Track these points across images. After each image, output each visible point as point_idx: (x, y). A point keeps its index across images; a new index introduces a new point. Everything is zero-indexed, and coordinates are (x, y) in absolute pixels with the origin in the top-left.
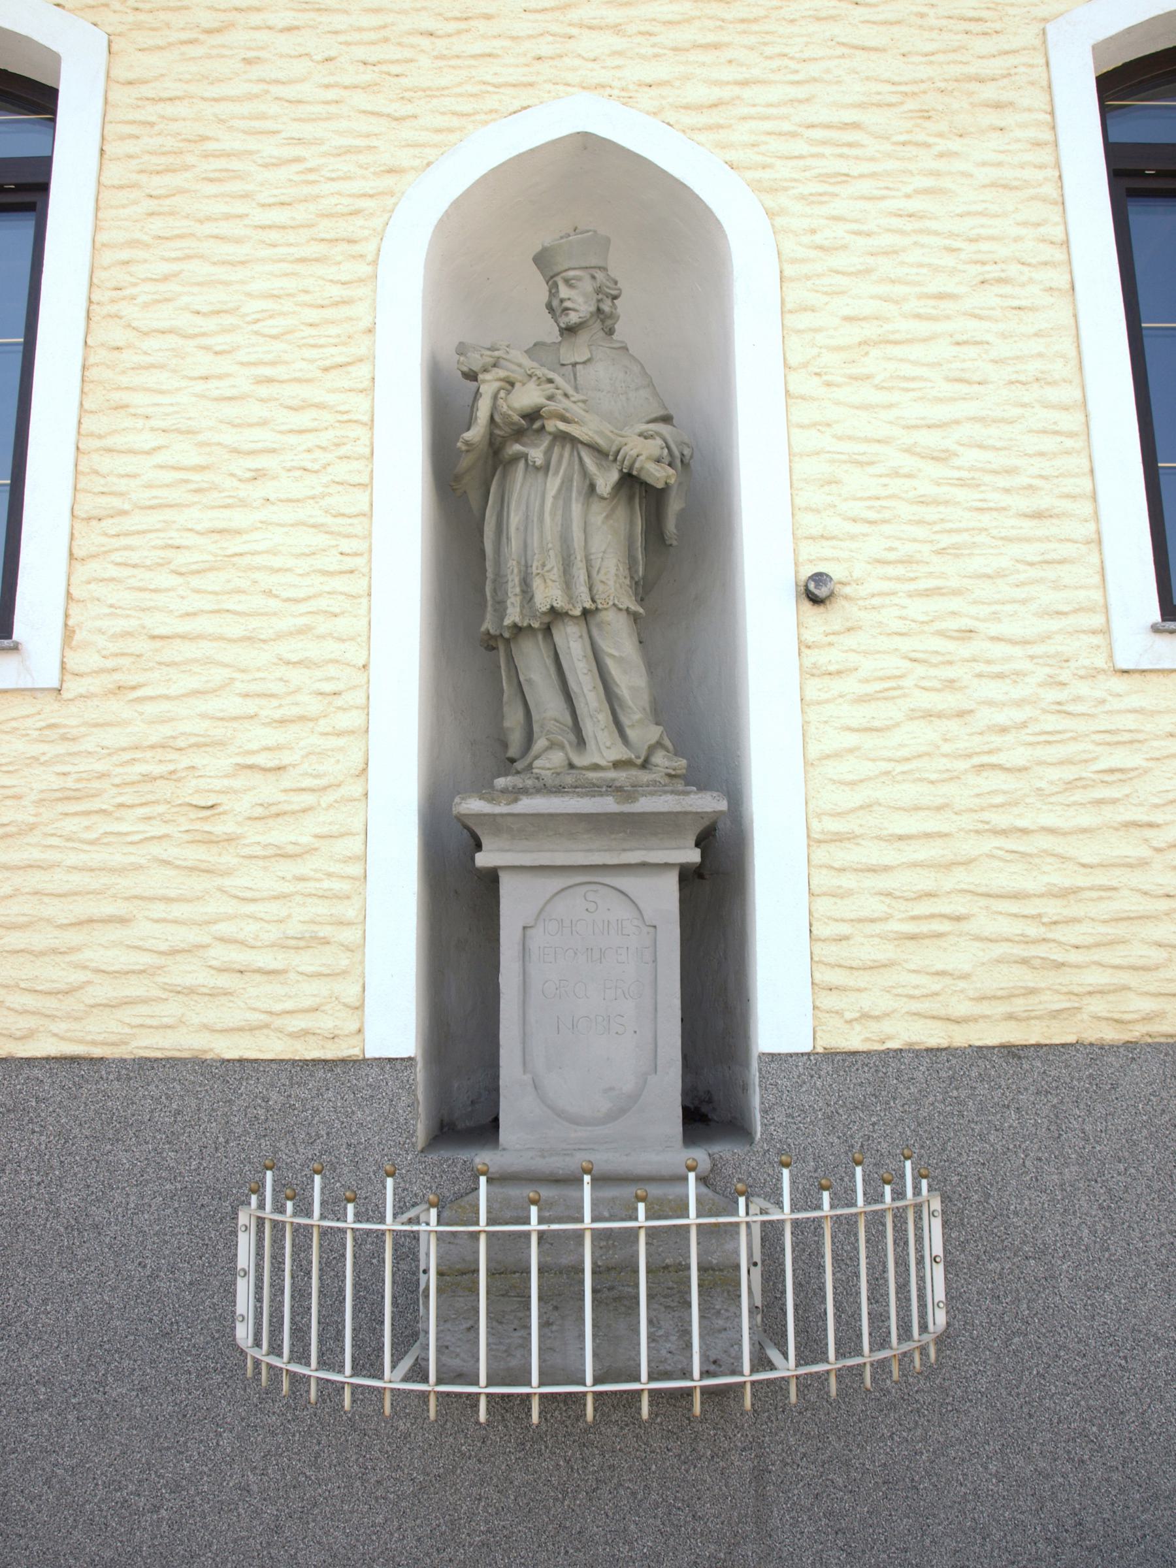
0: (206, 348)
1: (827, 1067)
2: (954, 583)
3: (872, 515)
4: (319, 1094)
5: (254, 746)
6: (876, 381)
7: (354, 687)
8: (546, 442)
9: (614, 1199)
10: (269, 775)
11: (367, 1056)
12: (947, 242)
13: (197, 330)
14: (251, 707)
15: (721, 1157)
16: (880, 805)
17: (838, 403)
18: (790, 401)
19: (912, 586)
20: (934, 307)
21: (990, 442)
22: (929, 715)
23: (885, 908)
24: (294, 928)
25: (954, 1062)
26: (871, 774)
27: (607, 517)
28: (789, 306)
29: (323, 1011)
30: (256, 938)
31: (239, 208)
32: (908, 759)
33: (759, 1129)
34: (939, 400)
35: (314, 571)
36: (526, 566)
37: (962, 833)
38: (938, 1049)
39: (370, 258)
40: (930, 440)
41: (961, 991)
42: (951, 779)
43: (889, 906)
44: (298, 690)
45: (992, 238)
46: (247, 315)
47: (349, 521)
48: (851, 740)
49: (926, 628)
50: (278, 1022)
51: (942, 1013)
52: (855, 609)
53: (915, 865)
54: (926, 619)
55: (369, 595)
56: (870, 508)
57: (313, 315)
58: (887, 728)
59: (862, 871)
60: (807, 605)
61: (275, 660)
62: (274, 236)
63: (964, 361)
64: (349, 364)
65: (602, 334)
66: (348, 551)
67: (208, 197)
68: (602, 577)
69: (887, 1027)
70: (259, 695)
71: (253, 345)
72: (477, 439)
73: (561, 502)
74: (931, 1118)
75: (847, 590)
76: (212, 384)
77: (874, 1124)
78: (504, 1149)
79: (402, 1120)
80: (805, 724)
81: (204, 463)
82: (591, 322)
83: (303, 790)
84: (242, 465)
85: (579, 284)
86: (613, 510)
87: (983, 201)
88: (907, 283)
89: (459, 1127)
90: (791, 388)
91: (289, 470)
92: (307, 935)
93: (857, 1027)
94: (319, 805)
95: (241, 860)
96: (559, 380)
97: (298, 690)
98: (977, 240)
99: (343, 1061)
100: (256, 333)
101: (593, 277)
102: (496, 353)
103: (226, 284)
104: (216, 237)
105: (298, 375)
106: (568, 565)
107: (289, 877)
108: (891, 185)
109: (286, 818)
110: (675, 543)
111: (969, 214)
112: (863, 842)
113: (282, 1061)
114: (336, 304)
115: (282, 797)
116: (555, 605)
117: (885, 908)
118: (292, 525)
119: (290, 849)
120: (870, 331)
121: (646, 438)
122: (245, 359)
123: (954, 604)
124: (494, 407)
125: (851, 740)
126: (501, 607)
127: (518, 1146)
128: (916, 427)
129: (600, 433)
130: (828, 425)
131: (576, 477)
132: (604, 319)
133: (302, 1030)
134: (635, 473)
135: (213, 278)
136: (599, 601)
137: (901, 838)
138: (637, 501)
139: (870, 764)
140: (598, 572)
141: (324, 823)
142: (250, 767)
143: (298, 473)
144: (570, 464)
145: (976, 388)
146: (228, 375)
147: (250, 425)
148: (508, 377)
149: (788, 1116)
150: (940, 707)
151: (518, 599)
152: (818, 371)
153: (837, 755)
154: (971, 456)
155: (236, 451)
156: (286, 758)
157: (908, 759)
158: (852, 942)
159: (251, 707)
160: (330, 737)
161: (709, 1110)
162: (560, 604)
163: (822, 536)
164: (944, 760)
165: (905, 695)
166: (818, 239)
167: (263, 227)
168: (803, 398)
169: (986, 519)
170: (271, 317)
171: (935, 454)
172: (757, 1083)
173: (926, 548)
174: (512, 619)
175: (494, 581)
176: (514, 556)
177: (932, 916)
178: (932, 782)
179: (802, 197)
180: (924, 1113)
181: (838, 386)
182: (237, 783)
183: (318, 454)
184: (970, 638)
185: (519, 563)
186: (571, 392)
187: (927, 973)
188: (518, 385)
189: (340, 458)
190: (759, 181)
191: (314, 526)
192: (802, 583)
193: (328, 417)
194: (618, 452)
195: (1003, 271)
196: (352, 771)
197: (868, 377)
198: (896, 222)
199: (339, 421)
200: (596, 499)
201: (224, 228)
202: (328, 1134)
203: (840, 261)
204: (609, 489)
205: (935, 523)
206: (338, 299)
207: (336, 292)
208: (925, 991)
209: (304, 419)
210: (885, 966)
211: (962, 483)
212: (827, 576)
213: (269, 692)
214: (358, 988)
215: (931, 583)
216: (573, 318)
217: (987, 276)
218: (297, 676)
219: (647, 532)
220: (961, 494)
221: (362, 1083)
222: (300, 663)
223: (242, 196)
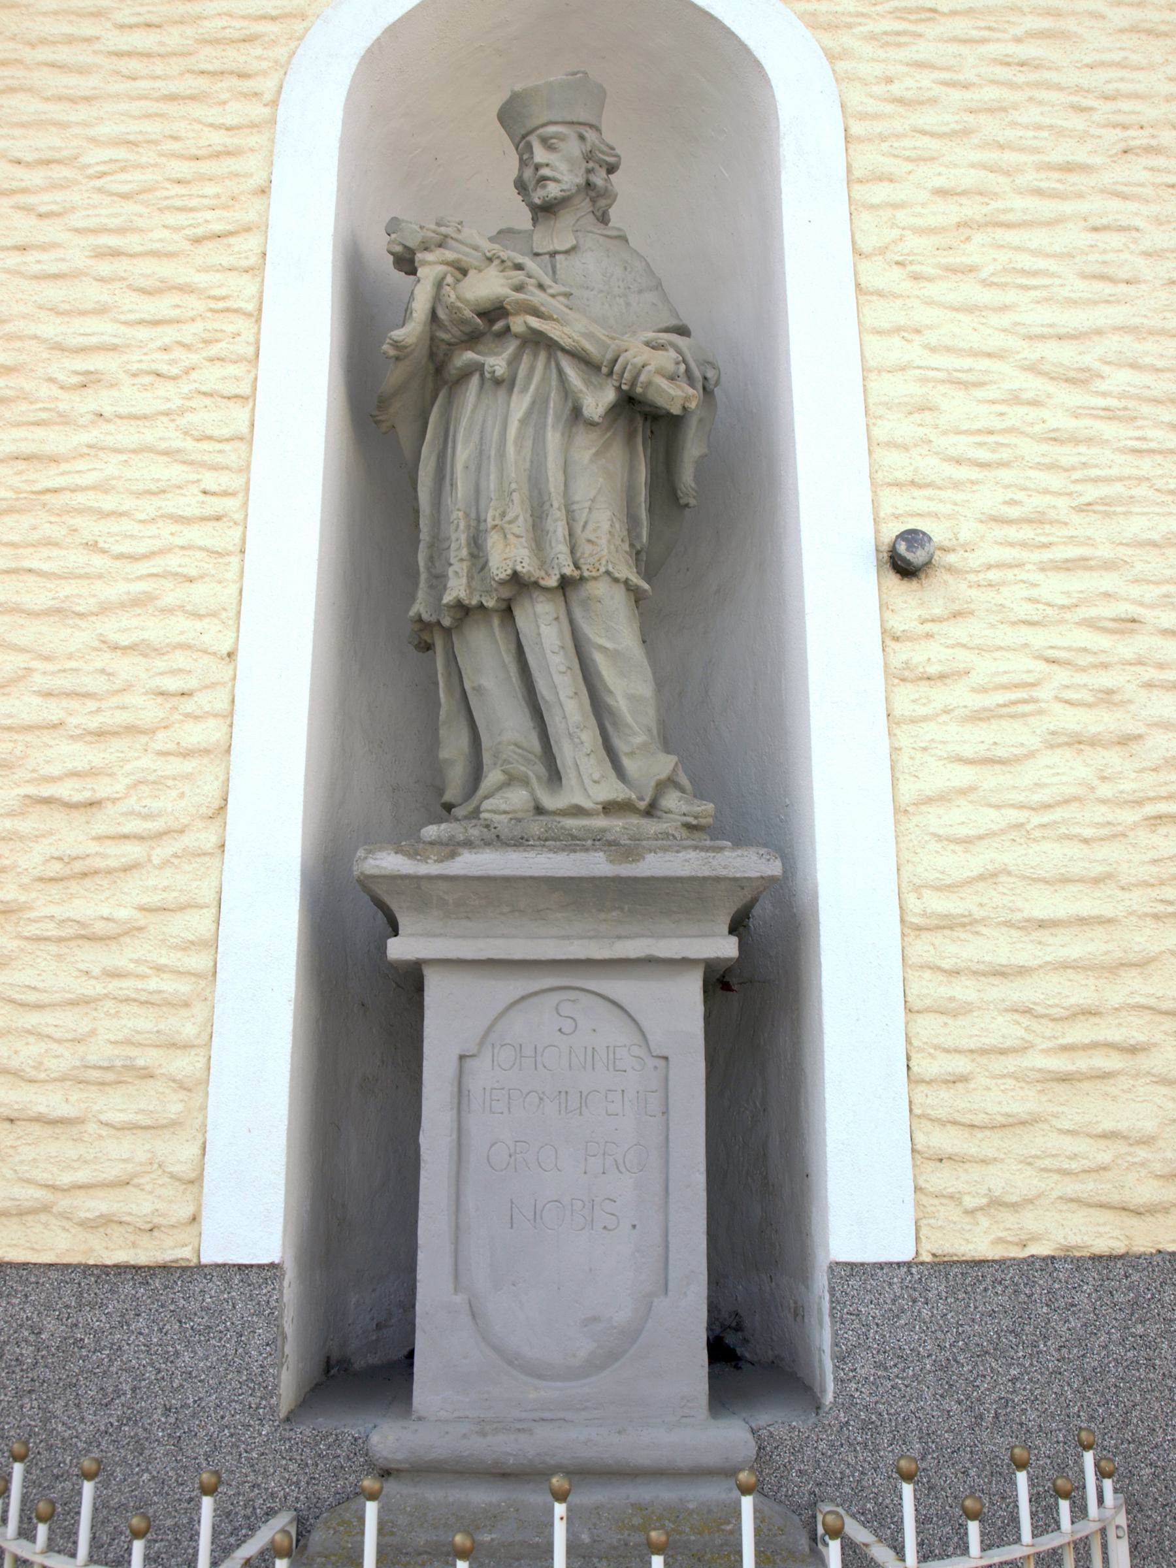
0: (28, 209)
1: (937, 1286)
2: (1105, 552)
3: (983, 455)
4: (124, 1323)
5: (55, 770)
6: (983, 275)
7: (213, 685)
8: (511, 347)
9: (598, 1508)
10: (75, 814)
11: (204, 1261)
12: (1074, 99)
13: (15, 185)
14: (54, 711)
15: (771, 1435)
16: (1009, 873)
17: (930, 303)
18: (862, 299)
19: (1046, 555)
20: (1059, 181)
21: (1148, 360)
22: (1078, 741)
23: (1021, 1033)
24: (99, 1051)
25: (1135, 1277)
26: (995, 827)
27: (596, 454)
28: (857, 174)
29: (137, 1186)
30: (39, 1066)
31: (88, 28)
32: (1048, 806)
33: (830, 1386)
34: (1071, 303)
35: (162, 516)
36: (478, 520)
37: (1134, 919)
38: (1110, 1257)
39: (268, 96)
40: (1063, 355)
41: (1142, 1164)
42: (1114, 836)
43: (1027, 1029)
44: (127, 688)
45: (1136, 96)
46: (89, 166)
47: (219, 446)
48: (963, 776)
49: (1068, 616)
50: (64, 1203)
51: (1116, 1198)
52: (963, 586)
53: (1065, 966)
54: (1066, 601)
55: (243, 552)
56: (980, 444)
57: (183, 169)
58: (1017, 760)
59: (984, 974)
60: (893, 579)
61: (96, 644)
62: (133, 65)
63: (1105, 252)
64: (231, 233)
65: (591, 218)
66: (213, 487)
67: (45, 14)
68: (589, 534)
69: (1030, 1221)
70: (68, 695)
71: (95, 207)
72: (411, 340)
73: (530, 431)
74: (1103, 1370)
75: (951, 558)
76: (31, 257)
77: (1014, 1380)
78: (420, 1419)
79: (255, 1368)
80: (895, 750)
81: (10, 362)
82: (576, 201)
83: (126, 837)
84: (66, 367)
85: (562, 145)
86: (606, 446)
87: (1121, 49)
88: (1022, 150)
89: (357, 1366)
90: (863, 280)
91: (134, 375)
92: (118, 1063)
93: (984, 1221)
94: (150, 861)
95: (22, 943)
96: (530, 264)
97: (127, 688)
98: (1114, 99)
99: (165, 1268)
100: (100, 190)
101: (582, 138)
102: (443, 230)
103: (64, 125)
104: (53, 65)
105: (157, 246)
106: (540, 518)
107: (96, 971)
108: (994, 25)
109: (97, 879)
110: (692, 502)
111: (1102, 64)
112: (984, 930)
113: (67, 1266)
114: (217, 155)
115: (93, 847)
116: (519, 568)
117: (1021, 1033)
118: (134, 451)
119: (100, 928)
120: (972, 209)
121: (653, 348)
122: (81, 224)
123: (1108, 581)
124: (437, 298)
125: (963, 776)
126: (439, 581)
127: (443, 1414)
128: (1042, 337)
129: (589, 336)
130: (918, 331)
131: (554, 396)
132: (595, 197)
133: (101, 1216)
134: (639, 390)
135: (44, 117)
136: (584, 568)
137: (1042, 924)
138: (639, 439)
139: (993, 813)
140: (584, 527)
141: (155, 888)
142: (47, 801)
143: (147, 379)
144: (545, 379)
145: (1123, 288)
146: (55, 245)
147: (83, 313)
148: (458, 261)
149: (878, 1365)
150: (1093, 730)
151: (465, 565)
152: (900, 259)
153: (942, 798)
154: (1120, 379)
155: (59, 347)
156: (103, 788)
157: (1048, 806)
158: (972, 1085)
159: (54, 711)
160: (171, 758)
161: (745, 1353)
162: (527, 567)
163: (913, 483)
164: (1103, 809)
165: (1041, 712)
166: (896, 89)
167: (119, 54)
168: (880, 294)
169: (1146, 465)
170: (123, 170)
171: (1071, 374)
172: (826, 1306)
173: (1062, 503)
174: (454, 594)
175: (431, 546)
176: (460, 505)
177: (1094, 1046)
178: (1086, 841)
179: (872, 37)
180: (1092, 1362)
181: (930, 279)
182: (24, 826)
183: (179, 353)
184: (1132, 631)
185: (467, 515)
186: (547, 281)
187: (1089, 1135)
188: (472, 273)
189: (211, 360)
190: (814, 14)
191: (166, 453)
192: (885, 548)
193: (195, 304)
194: (616, 361)
195: (1153, 136)
196: (203, 810)
197: (972, 269)
198: (1001, 72)
199: (212, 310)
200: (581, 429)
201: (64, 54)
202: (134, 1389)
203: (928, 118)
204: (601, 410)
205: (1074, 468)
206: (219, 148)
207: (218, 139)
208: (1086, 1164)
209: (162, 306)
210: (1023, 1123)
211: (1109, 414)
212: (924, 534)
213: (83, 690)
214: (195, 1150)
215: (1073, 552)
216: (553, 190)
217: (1132, 143)
218: (126, 667)
219: (652, 486)
220: (1109, 430)
221: (193, 1306)
222: (132, 647)
223: (92, 14)
